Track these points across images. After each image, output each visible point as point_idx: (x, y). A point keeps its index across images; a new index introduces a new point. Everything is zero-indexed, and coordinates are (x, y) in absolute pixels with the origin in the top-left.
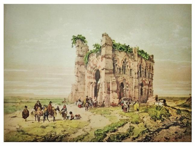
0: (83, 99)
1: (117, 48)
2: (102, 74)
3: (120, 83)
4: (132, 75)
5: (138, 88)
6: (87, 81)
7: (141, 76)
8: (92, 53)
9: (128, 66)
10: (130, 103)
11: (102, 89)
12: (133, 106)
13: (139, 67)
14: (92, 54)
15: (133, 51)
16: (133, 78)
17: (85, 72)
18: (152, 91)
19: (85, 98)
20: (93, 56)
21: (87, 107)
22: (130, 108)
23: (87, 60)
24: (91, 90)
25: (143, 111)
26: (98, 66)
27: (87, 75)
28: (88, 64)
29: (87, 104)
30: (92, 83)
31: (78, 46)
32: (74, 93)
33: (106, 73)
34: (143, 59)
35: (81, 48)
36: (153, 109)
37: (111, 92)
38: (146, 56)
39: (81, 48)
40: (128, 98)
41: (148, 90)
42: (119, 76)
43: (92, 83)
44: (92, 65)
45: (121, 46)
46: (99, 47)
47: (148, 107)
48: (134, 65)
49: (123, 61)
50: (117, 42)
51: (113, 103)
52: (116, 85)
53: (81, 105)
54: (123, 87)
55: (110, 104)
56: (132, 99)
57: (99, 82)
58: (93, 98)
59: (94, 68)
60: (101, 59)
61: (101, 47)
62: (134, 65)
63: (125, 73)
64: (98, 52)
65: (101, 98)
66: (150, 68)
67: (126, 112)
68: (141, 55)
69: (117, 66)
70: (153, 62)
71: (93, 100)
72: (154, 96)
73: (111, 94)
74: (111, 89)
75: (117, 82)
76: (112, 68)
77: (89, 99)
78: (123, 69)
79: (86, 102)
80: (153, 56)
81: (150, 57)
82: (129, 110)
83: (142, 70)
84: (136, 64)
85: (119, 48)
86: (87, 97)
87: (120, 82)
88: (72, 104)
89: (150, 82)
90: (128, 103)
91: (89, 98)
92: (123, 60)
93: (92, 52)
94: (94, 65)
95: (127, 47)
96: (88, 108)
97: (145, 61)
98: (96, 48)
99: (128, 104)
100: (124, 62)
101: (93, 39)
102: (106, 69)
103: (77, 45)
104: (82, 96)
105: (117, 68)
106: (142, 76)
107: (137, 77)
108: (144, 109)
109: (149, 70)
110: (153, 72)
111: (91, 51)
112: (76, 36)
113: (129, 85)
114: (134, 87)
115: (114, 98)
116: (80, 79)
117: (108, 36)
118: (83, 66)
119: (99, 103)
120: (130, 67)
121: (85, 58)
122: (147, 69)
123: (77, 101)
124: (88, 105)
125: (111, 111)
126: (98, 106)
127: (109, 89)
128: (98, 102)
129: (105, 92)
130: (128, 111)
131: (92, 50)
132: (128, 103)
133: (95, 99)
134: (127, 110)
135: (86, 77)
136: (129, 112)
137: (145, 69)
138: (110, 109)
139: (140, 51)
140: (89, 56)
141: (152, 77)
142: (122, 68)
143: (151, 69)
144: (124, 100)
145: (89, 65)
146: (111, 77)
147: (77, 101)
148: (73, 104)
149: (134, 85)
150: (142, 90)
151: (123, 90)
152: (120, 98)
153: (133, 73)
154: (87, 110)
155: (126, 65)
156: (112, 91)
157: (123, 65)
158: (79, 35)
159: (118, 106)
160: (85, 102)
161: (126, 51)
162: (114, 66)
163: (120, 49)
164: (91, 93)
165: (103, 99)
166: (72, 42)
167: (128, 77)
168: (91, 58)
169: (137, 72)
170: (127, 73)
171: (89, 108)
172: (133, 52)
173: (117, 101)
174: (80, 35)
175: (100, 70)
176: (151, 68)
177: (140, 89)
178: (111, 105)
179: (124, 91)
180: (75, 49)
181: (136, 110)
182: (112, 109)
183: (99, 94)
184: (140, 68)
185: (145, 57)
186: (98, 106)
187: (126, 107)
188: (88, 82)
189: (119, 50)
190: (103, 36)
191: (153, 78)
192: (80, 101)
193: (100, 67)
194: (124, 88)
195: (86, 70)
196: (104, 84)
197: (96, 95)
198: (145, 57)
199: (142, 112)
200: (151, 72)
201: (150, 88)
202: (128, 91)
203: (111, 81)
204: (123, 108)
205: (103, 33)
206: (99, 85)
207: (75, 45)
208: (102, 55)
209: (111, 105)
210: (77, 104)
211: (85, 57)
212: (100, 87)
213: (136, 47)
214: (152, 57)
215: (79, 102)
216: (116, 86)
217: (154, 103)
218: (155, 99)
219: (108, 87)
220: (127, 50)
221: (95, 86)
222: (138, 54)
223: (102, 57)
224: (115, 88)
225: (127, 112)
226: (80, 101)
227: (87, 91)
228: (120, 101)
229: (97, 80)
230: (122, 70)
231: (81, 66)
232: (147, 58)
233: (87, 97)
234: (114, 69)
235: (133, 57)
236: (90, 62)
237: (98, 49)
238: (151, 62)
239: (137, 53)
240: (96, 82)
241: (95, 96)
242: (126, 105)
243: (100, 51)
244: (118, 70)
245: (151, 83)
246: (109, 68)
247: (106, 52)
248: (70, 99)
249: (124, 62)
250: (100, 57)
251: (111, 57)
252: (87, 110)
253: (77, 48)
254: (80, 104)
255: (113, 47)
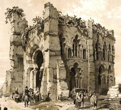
0: (22, 90)
1: (64, 22)
2: (46, 56)
3: (70, 68)
4: (86, 57)
5: (95, 75)
6: (27, 66)
7: (98, 59)
8: (31, 29)
9: (80, 45)
10: (85, 96)
11: (47, 78)
12: (89, 99)
13: (95, 46)
14: (32, 31)
15: (87, 25)
16: (88, 61)
17: (23, 55)
18: (113, 78)
19: (24, 89)
20: (33, 33)
21: (26, 101)
22: (85, 103)
23: (26, 39)
24: (32, 78)
25: (102, 106)
26: (40, 46)
27: (26, 58)
28: (27, 44)
29: (26, 97)
30: (33, 69)
31: (14, 21)
32: (9, 84)
33: (50, 56)
34: (100, 36)
35: (18, 24)
36: (116, 104)
37: (58, 81)
38: (104, 32)
39: (18, 24)
40: (82, 88)
41: (108, 77)
42: (69, 60)
43: (33, 69)
44: (32, 45)
45: (70, 19)
46: (41, 21)
47: (108, 101)
48: (87, 44)
49: (73, 39)
50: (63, 14)
51: (61, 95)
52: (65, 71)
53: (18, 99)
54: (75, 74)
55: (57, 97)
56: (87, 90)
57: (41, 68)
58: (35, 89)
59: (36, 49)
60: (44, 37)
61: (43, 22)
62: (88, 44)
63: (76, 55)
64: (40, 28)
65: (45, 89)
66: (110, 49)
67: (80, 108)
68: (98, 31)
69: (66, 47)
70: (113, 39)
71: (35, 92)
72: (117, 86)
73: (58, 84)
74: (58, 77)
75: (66, 67)
76: (59, 48)
77: (29, 90)
78: (73, 50)
79: (26, 95)
80: (113, 31)
81: (109, 33)
82: (83, 105)
83: (99, 50)
84: (90, 42)
85: (67, 22)
86: (27, 87)
87: (70, 67)
88: (7, 98)
89: (110, 67)
90: (82, 95)
91: (28, 89)
92: (73, 38)
93: (31, 28)
94: (35, 45)
95: (78, 20)
96: (28, 102)
97: (103, 38)
98: (36, 23)
99: (82, 97)
100: (74, 41)
101: (33, 13)
102: (51, 51)
103: (12, 20)
104: (20, 86)
105: (66, 49)
106: (99, 58)
107: (93, 61)
108: (104, 103)
109: (108, 50)
110: (114, 53)
111: (30, 27)
112: (12, 8)
113: (82, 71)
114: (89, 73)
115: (62, 89)
116: (17, 63)
117: (52, 7)
118: (20, 48)
119: (43, 96)
120: (82, 47)
121: (23, 37)
122: (106, 49)
123: (14, 93)
124: (28, 99)
125: (59, 107)
126: (41, 99)
127: (55, 77)
128: (42, 95)
129: (50, 81)
130: (82, 106)
131: (32, 25)
132: (82, 95)
133: (38, 90)
134: (80, 106)
135: (25, 62)
136: (83, 108)
137: (104, 50)
138: (57, 104)
139: (95, 25)
140: (28, 33)
141: (113, 59)
142: (72, 48)
143: (111, 49)
144: (77, 91)
145: (28, 46)
146: (58, 60)
147: (14, 93)
148: (9, 98)
149: (89, 70)
150: (99, 77)
151: (75, 78)
152: (70, 89)
153: (88, 54)
154: (26, 106)
155: (77, 45)
156: (60, 80)
157: (73, 44)
158: (14, 7)
159: (68, 100)
160: (24, 94)
161: (77, 26)
162: (61, 46)
163: (69, 23)
164: (30, 81)
165: (48, 90)
166: (6, 16)
167: (81, 61)
168: (30, 37)
169: (92, 52)
170: (79, 55)
171: (29, 103)
172: (86, 27)
173: (66, 93)
174: (16, 6)
175: (43, 51)
176: (111, 47)
177: (98, 75)
178: (59, 99)
179: (76, 79)
180: (10, 25)
181: (93, 105)
182: (60, 104)
183: (42, 83)
184: (96, 48)
185: (103, 33)
186: (41, 99)
187: (79, 102)
188: (27, 68)
189: (68, 24)
190: (45, 7)
191: (115, 61)
192: (17, 92)
193: (42, 47)
194: (76, 76)
195: (24, 52)
196: (48, 70)
197: (38, 84)
198: (103, 33)
199: (101, 108)
200: (111, 54)
201: (110, 75)
202: (82, 80)
203: (57, 66)
204: (75, 103)
205: (46, 2)
206: (42, 72)
207: (10, 20)
208: (45, 31)
209: (59, 99)
210: (14, 97)
211: (22, 36)
212: (43, 75)
213: (90, 20)
214: (111, 33)
215: (16, 95)
216: (65, 72)
217: (117, 96)
218: (118, 89)
219: (54, 75)
220: (79, 25)
221: (37, 73)
222: (93, 29)
223: (45, 35)
224: (64, 75)
225: (81, 108)
226: (17, 92)
227: (26, 80)
228: (71, 92)
229: (40, 66)
230: (72, 51)
231: (17, 46)
232: (105, 34)
233: (27, 87)
234: (62, 50)
235: (86, 33)
236: (30, 41)
237: (39, 25)
238: (109, 40)
239: (92, 28)
240: (37, 67)
241: (36, 87)
242: (79, 98)
243: (43, 27)
244: (67, 52)
245: (111, 68)
246: (55, 49)
247: (50, 27)
248: (4, 90)
249: (76, 40)
250: (43, 34)
251: (56, 34)
252: (26, 106)
253: (13, 23)
254: (17, 98)
255: (59, 21)
